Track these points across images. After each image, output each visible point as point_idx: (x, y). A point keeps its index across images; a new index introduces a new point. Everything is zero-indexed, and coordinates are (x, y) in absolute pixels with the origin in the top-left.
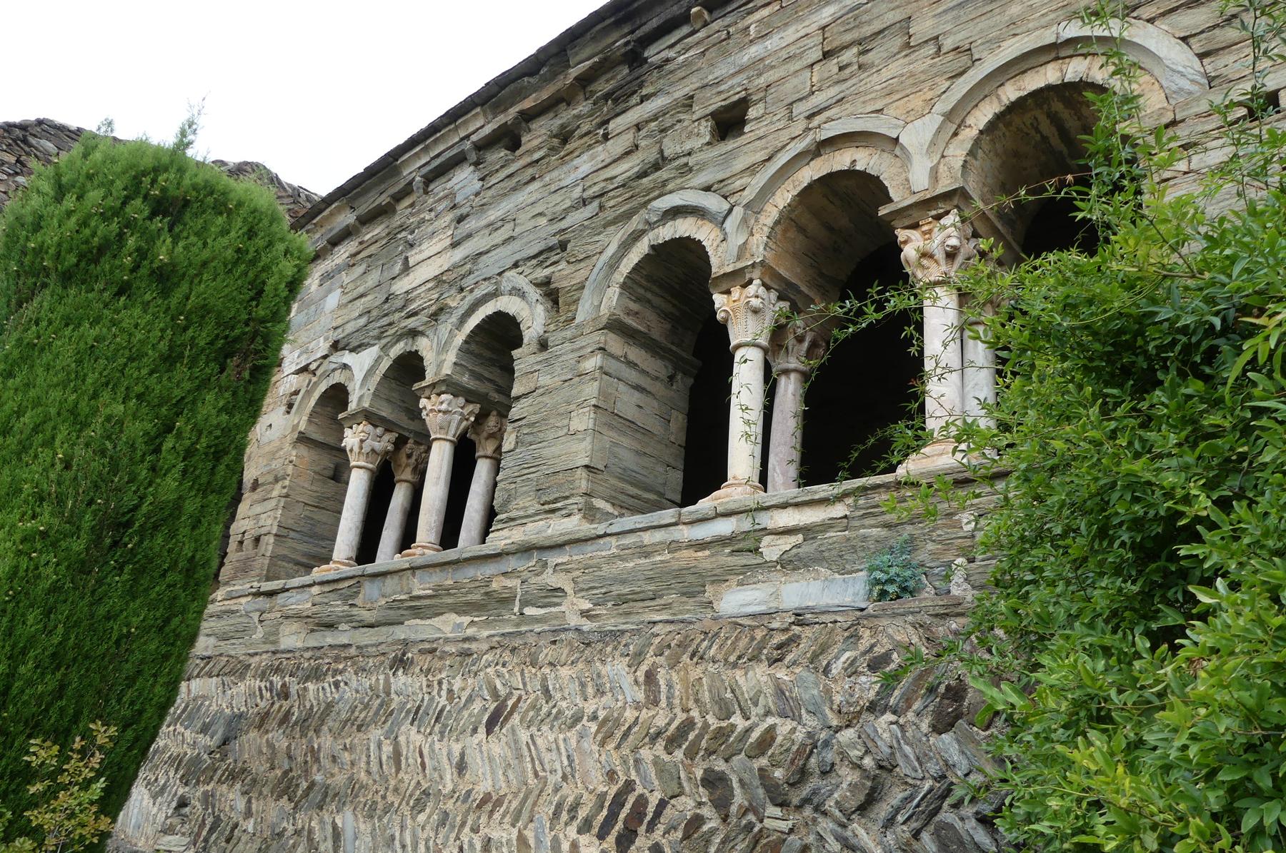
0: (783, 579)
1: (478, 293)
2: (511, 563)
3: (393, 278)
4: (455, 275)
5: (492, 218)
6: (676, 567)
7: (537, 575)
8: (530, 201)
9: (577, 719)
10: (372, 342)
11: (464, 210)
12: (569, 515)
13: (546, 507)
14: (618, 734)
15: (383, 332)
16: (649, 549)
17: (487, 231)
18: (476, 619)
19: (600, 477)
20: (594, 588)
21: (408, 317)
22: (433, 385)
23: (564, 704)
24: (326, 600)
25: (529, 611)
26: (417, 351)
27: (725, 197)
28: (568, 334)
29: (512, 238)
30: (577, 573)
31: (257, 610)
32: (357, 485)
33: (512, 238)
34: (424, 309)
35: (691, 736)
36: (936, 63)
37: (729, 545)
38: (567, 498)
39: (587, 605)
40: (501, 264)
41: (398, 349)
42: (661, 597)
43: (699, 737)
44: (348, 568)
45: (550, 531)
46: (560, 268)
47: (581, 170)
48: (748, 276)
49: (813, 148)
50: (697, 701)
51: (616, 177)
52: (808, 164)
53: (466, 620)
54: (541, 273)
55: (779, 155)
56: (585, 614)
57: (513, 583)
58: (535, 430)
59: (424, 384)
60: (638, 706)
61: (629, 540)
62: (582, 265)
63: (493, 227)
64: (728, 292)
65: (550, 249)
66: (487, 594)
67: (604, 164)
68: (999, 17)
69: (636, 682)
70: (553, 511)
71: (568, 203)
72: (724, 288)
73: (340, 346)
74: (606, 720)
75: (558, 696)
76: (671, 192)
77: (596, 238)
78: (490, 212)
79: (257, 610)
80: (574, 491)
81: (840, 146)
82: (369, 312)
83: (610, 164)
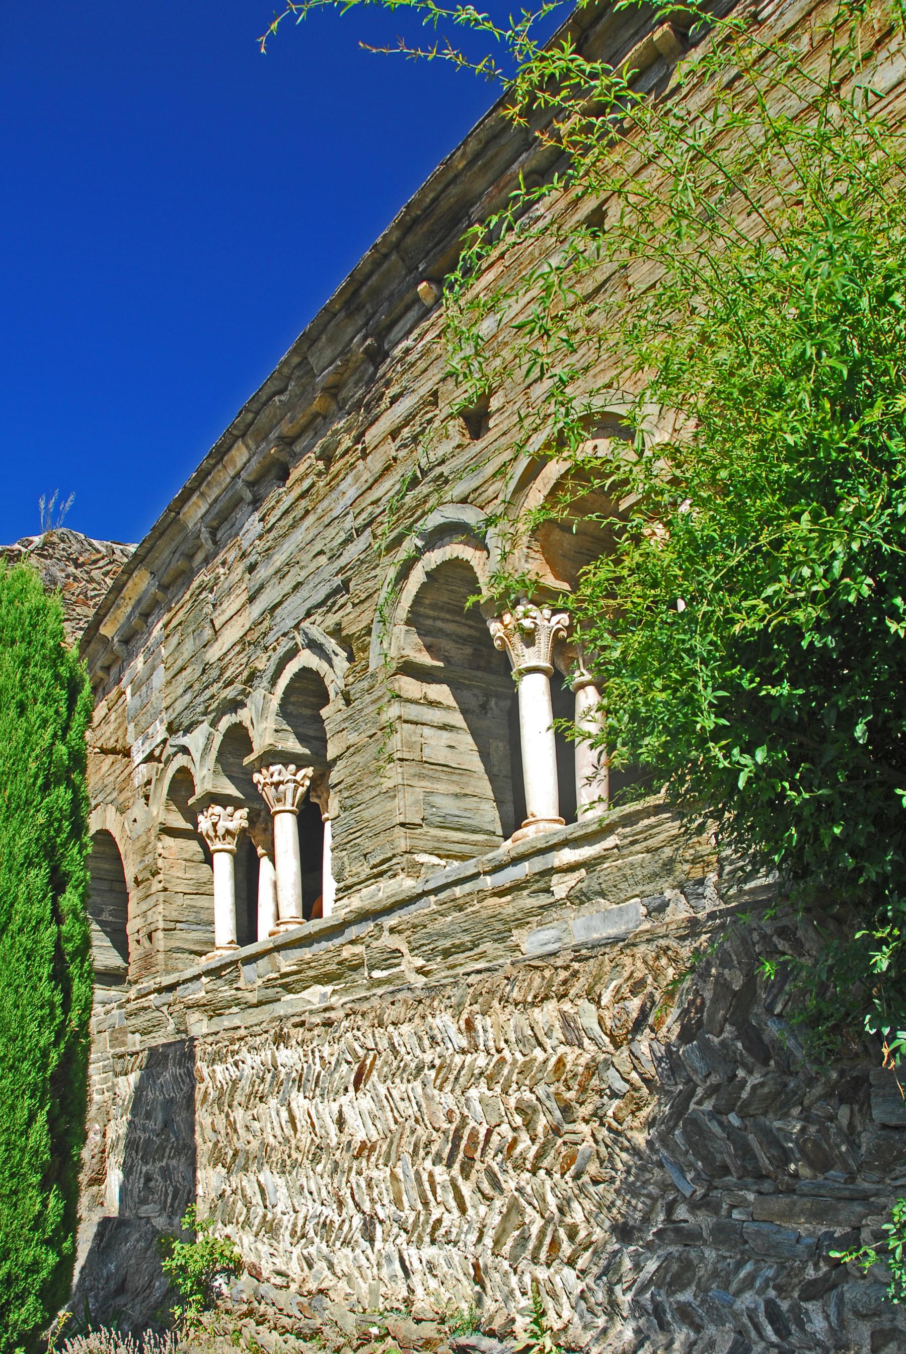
1: (281, 651)
2: (352, 932)
3: (205, 646)
4: (257, 635)
5: (278, 564)
6: (485, 916)
8: (309, 538)
9: (419, 1069)
10: (201, 719)
11: (252, 559)
12: (395, 876)
13: (375, 870)
14: (452, 1077)
15: (207, 707)
16: (461, 901)
17: (275, 580)
18: (337, 988)
19: (419, 831)
21: (225, 687)
22: (260, 758)
23: (409, 1057)
24: (215, 987)
25: (377, 974)
26: (241, 722)
28: (365, 684)
29: (297, 586)
30: (408, 933)
31: (164, 1004)
32: (223, 865)
33: (297, 586)
34: (237, 676)
35: (505, 1072)
38: (390, 859)
39: (420, 962)
40: (294, 615)
41: (226, 722)
42: (478, 946)
43: (511, 1072)
44: (232, 952)
45: (381, 894)
46: (348, 611)
47: (348, 495)
50: (506, 1041)
51: (380, 499)
53: (329, 989)
54: (331, 620)
56: (420, 971)
57: (359, 949)
58: (354, 792)
59: (253, 757)
60: (463, 1052)
61: (442, 896)
62: (366, 605)
63: (281, 574)
65: (335, 592)
66: (340, 963)
67: (368, 485)
69: (459, 1029)
70: (381, 874)
71: (343, 536)
73: (175, 726)
74: (441, 1067)
75: (403, 1050)
76: (431, 510)
77: (373, 573)
78: (276, 557)
79: (164, 1004)
80: (395, 852)
82: (191, 687)
83: (373, 485)
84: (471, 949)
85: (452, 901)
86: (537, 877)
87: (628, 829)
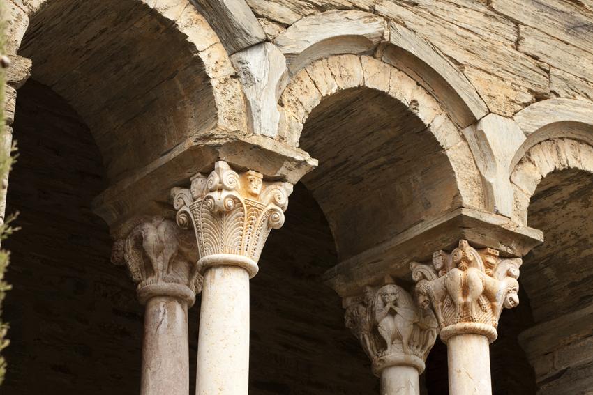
27: (257, 16)
36: (517, 57)
48: (282, 171)
49: (375, 41)
52: (360, 55)
55: (337, 15)
64: (240, 171)
68: (572, 58)
72: (241, 162)
81: (401, 66)
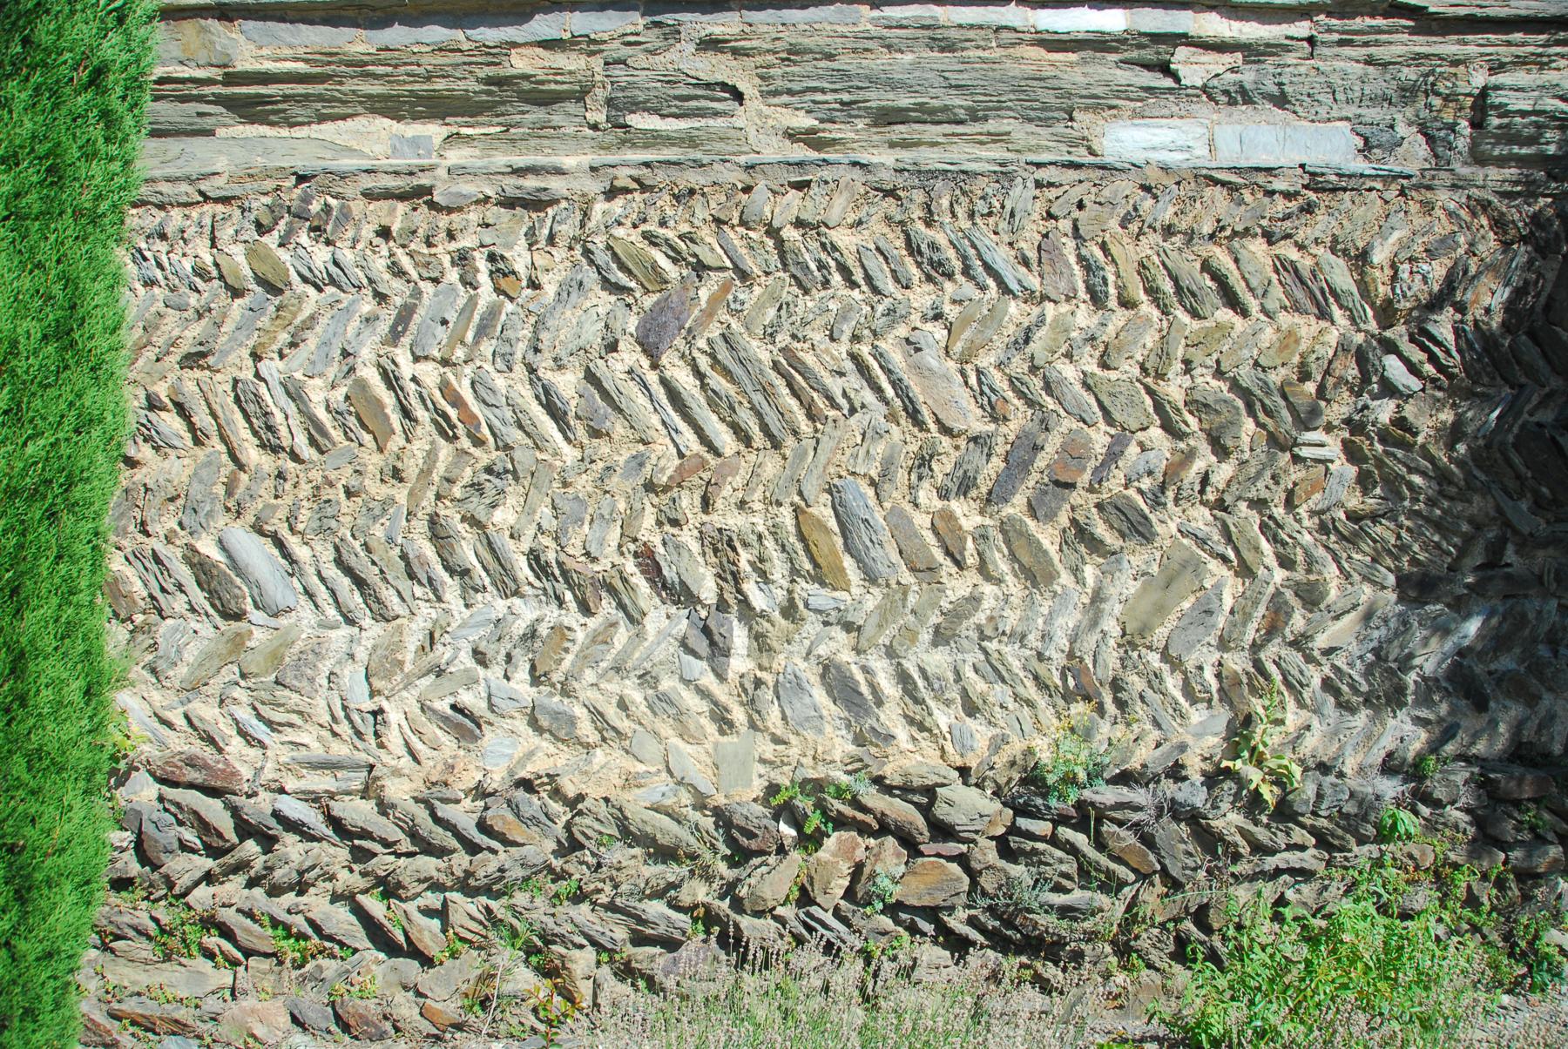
0: (1215, 117)
6: (1017, 73)
7: (652, 52)
16: (954, 34)
20: (815, 90)
37: (1115, 50)
84: (961, 122)
85: (928, 27)
86: (1144, 40)
87: (1334, 21)
